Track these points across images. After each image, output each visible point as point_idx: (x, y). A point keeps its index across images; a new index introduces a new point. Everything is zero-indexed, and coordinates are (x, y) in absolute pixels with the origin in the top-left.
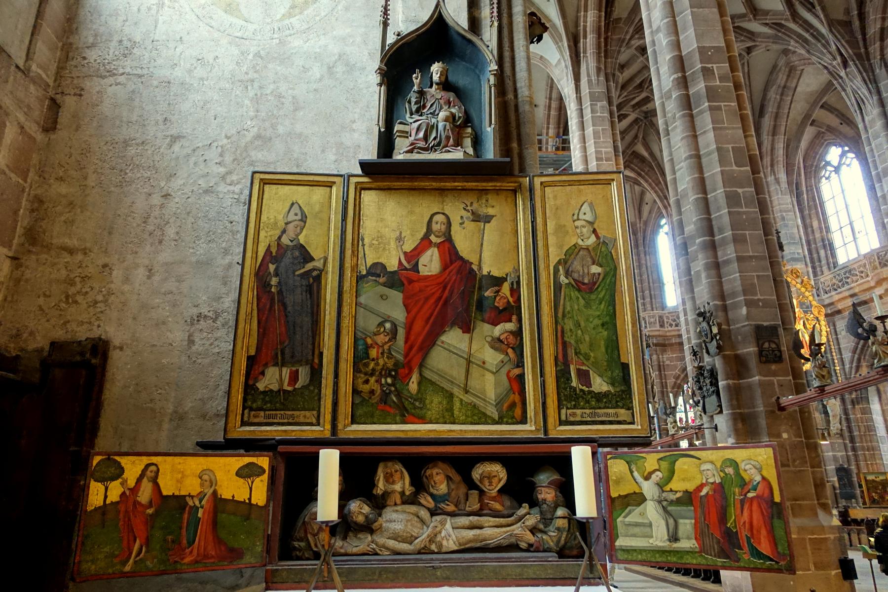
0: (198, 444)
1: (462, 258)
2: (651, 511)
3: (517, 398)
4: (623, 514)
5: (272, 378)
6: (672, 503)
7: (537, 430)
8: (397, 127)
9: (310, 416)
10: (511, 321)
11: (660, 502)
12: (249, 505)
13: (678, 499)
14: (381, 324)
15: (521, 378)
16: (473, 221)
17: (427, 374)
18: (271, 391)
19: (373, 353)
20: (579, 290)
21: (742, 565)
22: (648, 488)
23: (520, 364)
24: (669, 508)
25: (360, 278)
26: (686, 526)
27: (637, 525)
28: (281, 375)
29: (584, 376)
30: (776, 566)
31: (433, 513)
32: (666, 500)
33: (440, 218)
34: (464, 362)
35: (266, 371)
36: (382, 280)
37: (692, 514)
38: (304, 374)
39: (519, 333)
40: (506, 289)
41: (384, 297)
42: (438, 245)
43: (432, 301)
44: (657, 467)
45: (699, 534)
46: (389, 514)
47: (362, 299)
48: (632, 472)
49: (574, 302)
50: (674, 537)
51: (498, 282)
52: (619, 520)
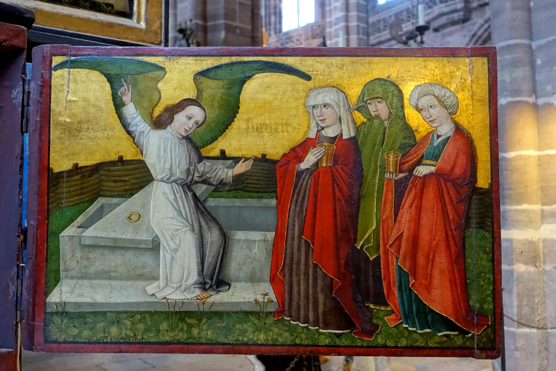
2: (162, 210)
4: (81, 219)
6: (219, 188)
11: (188, 186)
13: (238, 178)
21: (380, 340)
22: (162, 151)
24: (211, 203)
26: (252, 248)
27: (116, 246)
30: (459, 342)
32: (204, 182)
37: (271, 218)
44: (192, 94)
45: (281, 271)
48: (118, 105)
50: (215, 277)
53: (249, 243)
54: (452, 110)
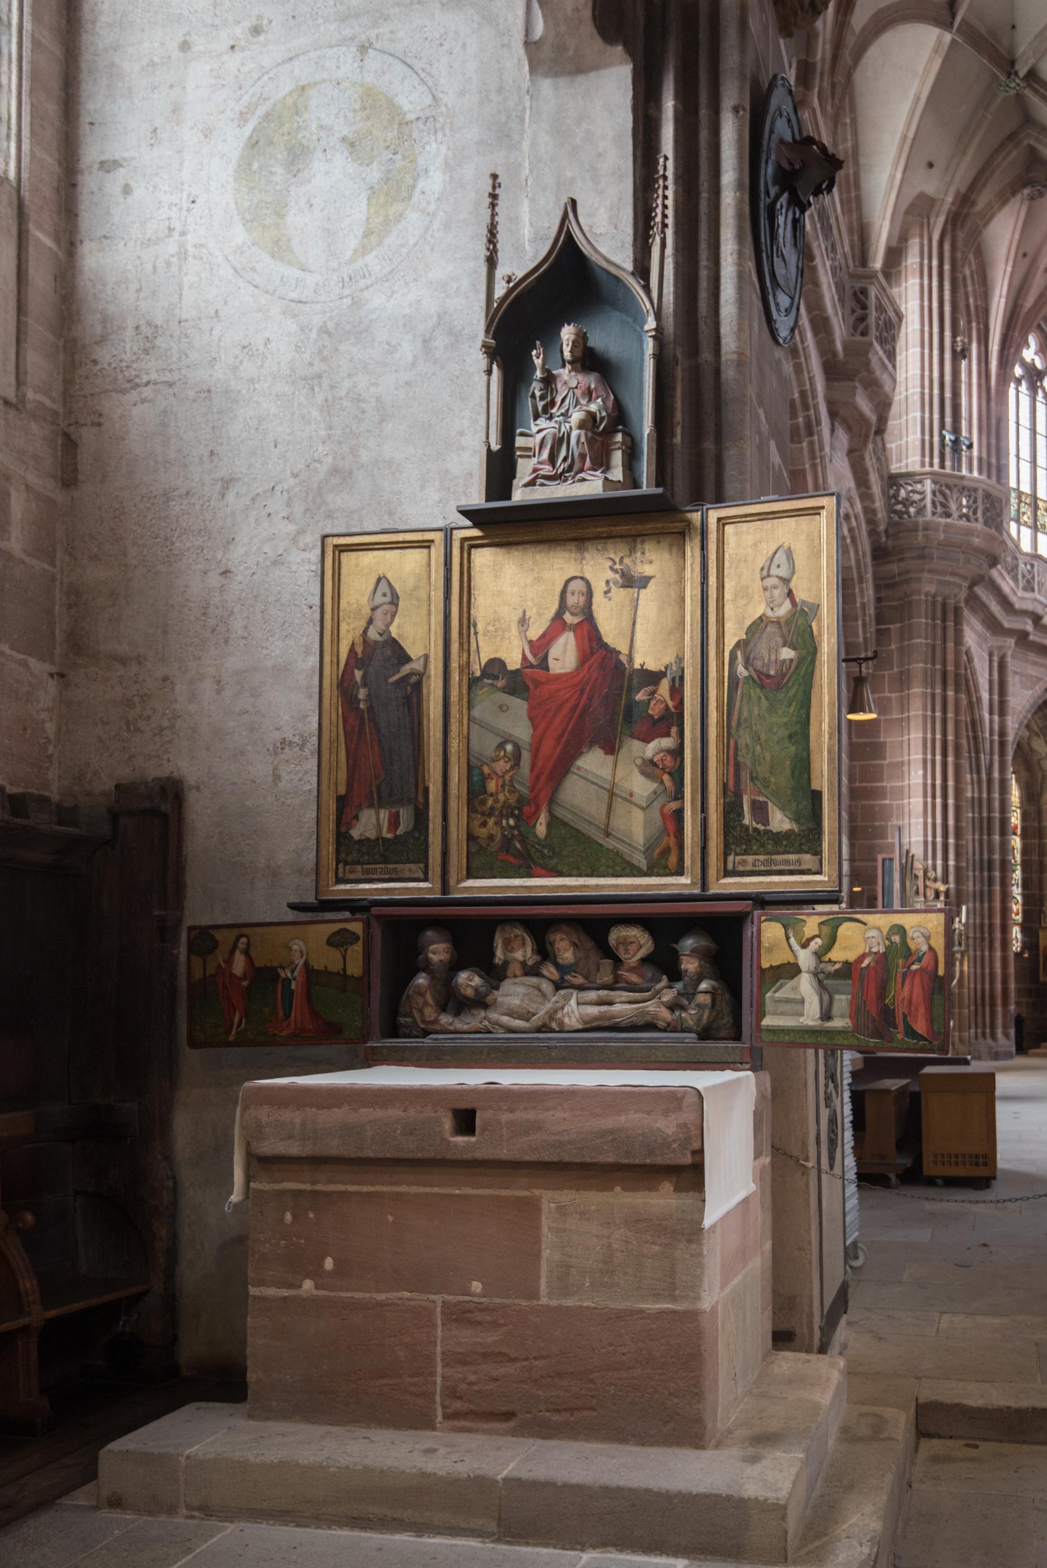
0: (293, 907)
1: (605, 646)
2: (805, 985)
3: (673, 841)
4: (773, 989)
5: (369, 823)
6: (829, 976)
7: (693, 883)
8: (520, 442)
9: (416, 869)
10: (668, 735)
12: (344, 975)
13: (836, 971)
14: (501, 746)
15: (679, 814)
16: (624, 586)
17: (559, 812)
18: (368, 839)
19: (492, 786)
20: (762, 687)
21: (895, 1045)
22: (805, 958)
23: (679, 795)
24: (825, 982)
25: (473, 683)
26: (842, 1002)
27: (787, 1001)
28: (378, 819)
29: (760, 811)
30: (929, 1047)
31: (558, 986)
32: (823, 972)
33: (577, 586)
34: (605, 795)
35: (360, 814)
36: (500, 683)
37: (850, 989)
38: (406, 816)
39: (678, 752)
40: (664, 688)
41: (504, 708)
42: (575, 628)
43: (565, 710)
44: (817, 933)
45: (856, 1011)
46: (507, 986)
47: (476, 713)
48: (788, 938)
49: (754, 707)
50: (827, 1015)
51: (653, 678)
52: (769, 995)
53: (841, 1000)
54: (928, 938)
